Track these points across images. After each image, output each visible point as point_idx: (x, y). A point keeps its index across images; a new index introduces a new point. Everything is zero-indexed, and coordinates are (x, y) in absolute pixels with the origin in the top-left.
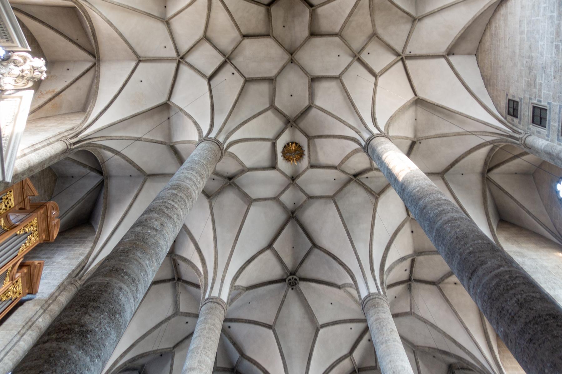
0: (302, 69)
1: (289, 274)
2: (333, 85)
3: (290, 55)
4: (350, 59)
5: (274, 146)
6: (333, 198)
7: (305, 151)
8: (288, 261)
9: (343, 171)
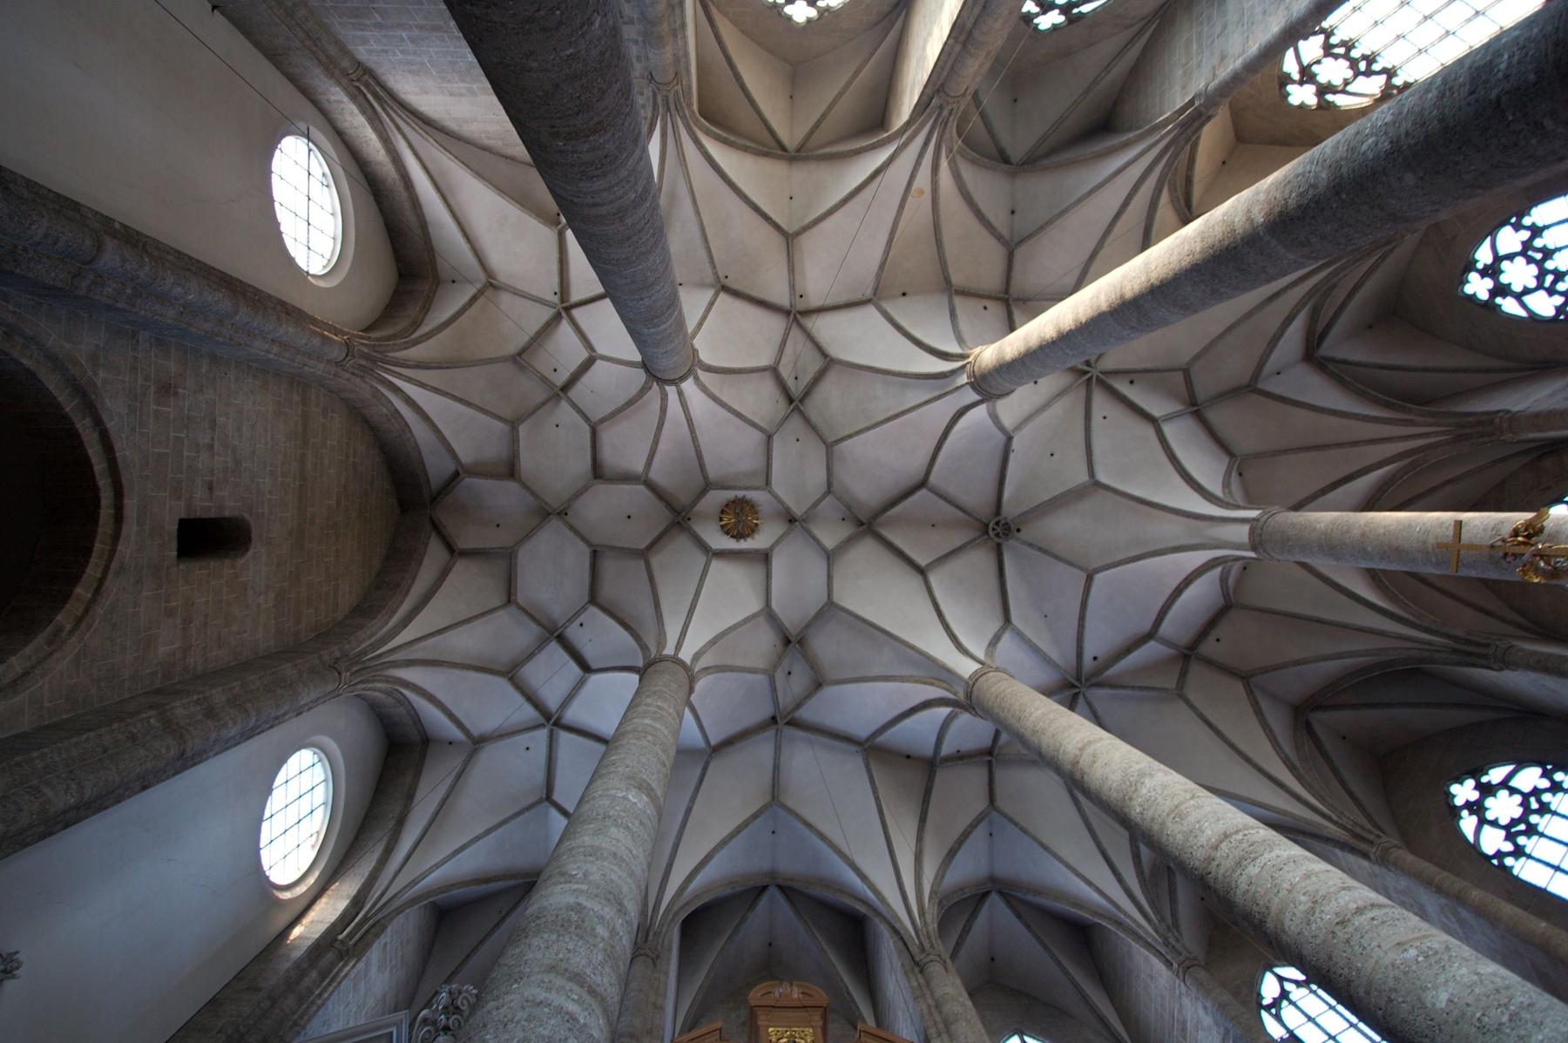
0: (578, 495)
1: (986, 537)
2: (608, 436)
3: (551, 517)
4: (564, 404)
5: (722, 554)
6: (830, 447)
8: (958, 539)
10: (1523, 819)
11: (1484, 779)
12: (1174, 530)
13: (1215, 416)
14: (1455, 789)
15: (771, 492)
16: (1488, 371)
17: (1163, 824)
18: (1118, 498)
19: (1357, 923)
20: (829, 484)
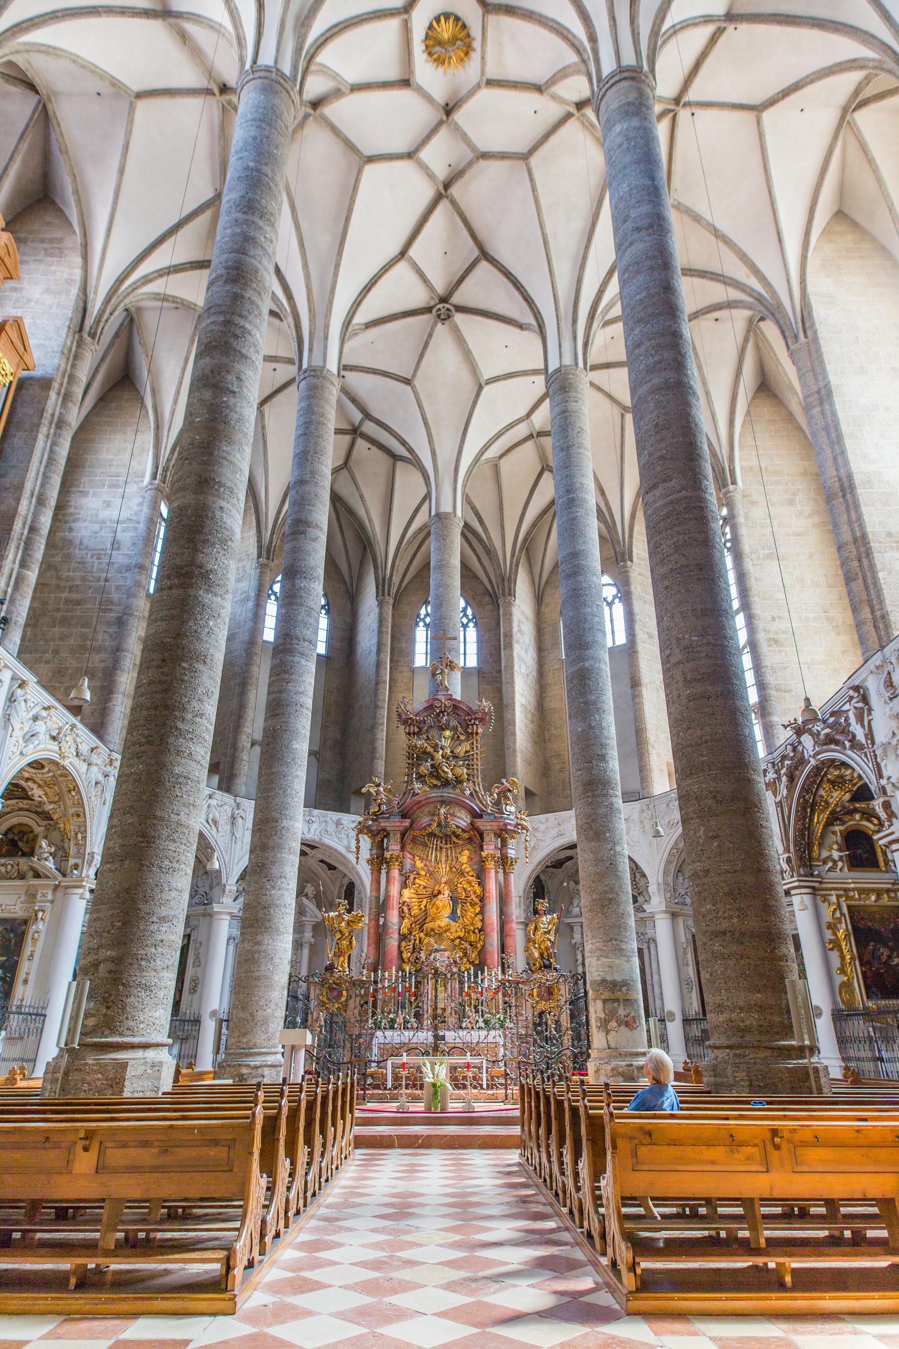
5: (406, 29)
6: (525, 157)
7: (474, 39)
9: (554, 97)
12: (446, 452)
13: (529, 445)
15: (478, 87)
16: (540, 577)
17: (301, 605)
18: (471, 402)
20: (485, 156)
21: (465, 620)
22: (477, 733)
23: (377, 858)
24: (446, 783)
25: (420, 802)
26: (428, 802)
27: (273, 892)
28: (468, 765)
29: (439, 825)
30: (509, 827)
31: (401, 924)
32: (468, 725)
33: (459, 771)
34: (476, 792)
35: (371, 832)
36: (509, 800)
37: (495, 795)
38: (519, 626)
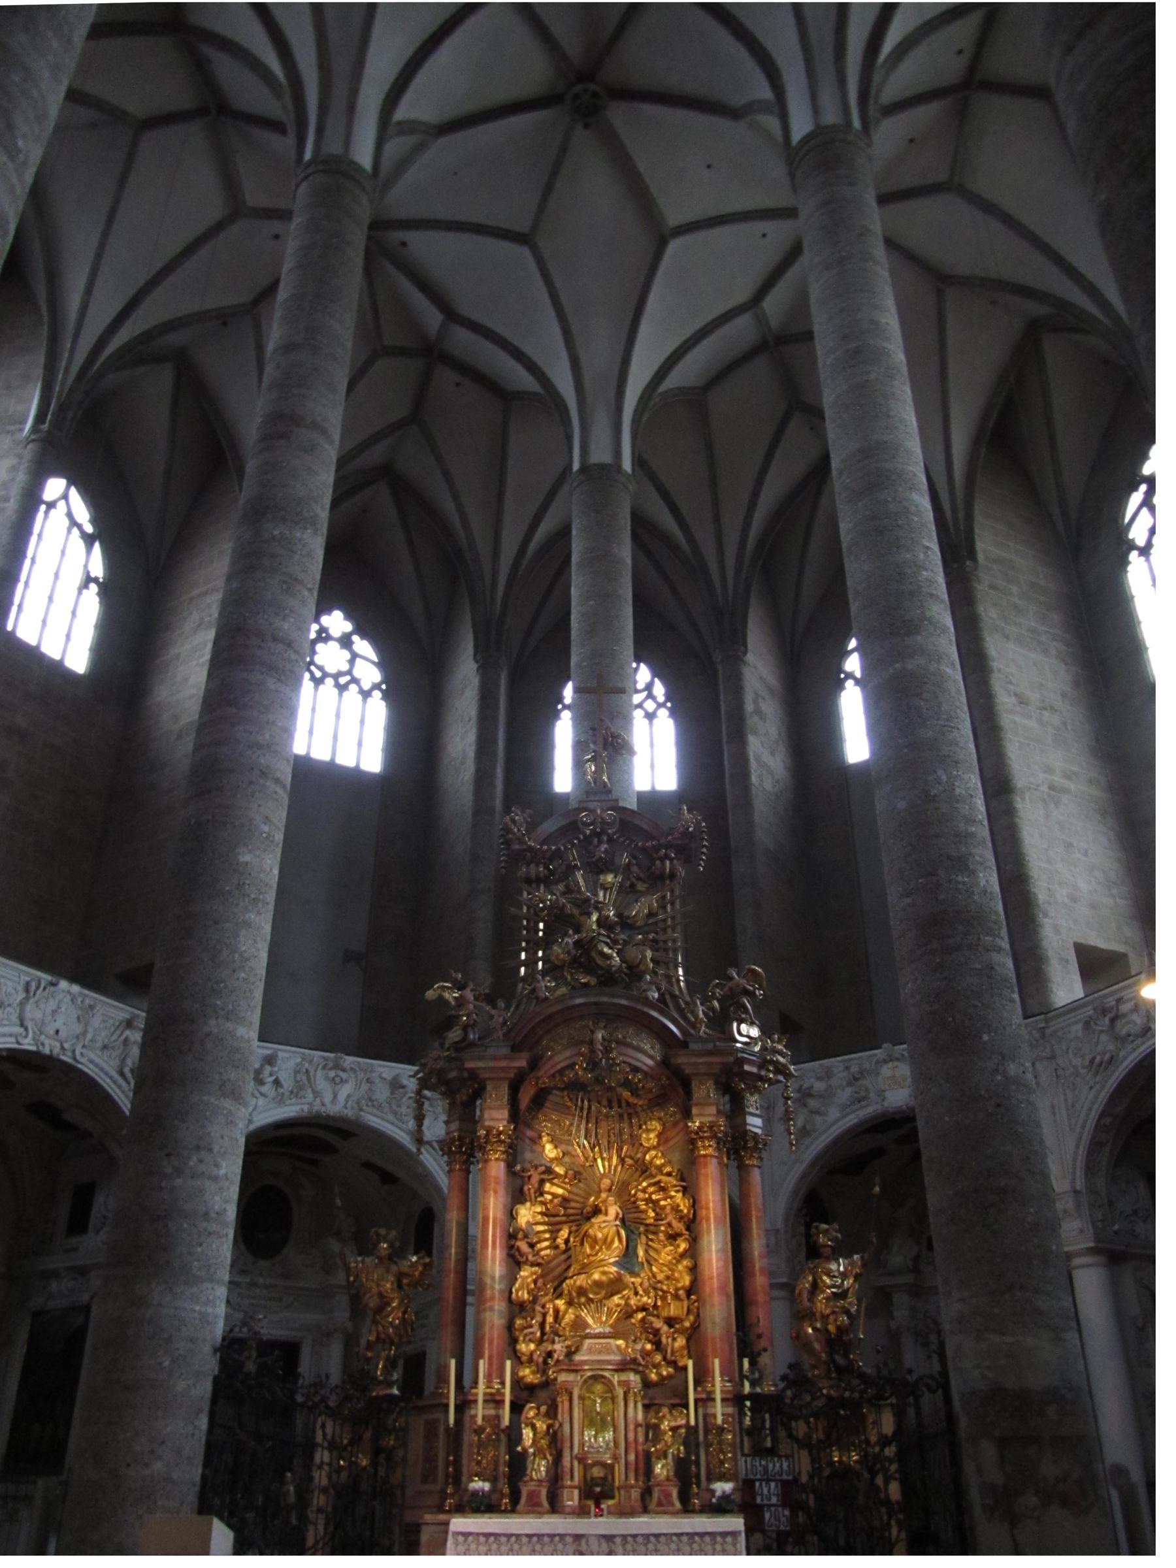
10: (325, 675)
11: (355, 638)
14: (338, 615)
19: (268, 783)
21: (650, 706)
22: (672, 876)
23: (460, 1138)
24: (608, 979)
25: (550, 1017)
26: (568, 1016)
27: (178, 1182)
28: (655, 941)
29: (593, 1064)
30: (747, 1068)
31: (511, 1278)
32: (653, 861)
33: (633, 953)
34: (674, 996)
35: (448, 1083)
36: (746, 1011)
37: (716, 1003)
38: (755, 702)
